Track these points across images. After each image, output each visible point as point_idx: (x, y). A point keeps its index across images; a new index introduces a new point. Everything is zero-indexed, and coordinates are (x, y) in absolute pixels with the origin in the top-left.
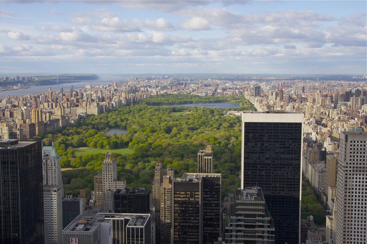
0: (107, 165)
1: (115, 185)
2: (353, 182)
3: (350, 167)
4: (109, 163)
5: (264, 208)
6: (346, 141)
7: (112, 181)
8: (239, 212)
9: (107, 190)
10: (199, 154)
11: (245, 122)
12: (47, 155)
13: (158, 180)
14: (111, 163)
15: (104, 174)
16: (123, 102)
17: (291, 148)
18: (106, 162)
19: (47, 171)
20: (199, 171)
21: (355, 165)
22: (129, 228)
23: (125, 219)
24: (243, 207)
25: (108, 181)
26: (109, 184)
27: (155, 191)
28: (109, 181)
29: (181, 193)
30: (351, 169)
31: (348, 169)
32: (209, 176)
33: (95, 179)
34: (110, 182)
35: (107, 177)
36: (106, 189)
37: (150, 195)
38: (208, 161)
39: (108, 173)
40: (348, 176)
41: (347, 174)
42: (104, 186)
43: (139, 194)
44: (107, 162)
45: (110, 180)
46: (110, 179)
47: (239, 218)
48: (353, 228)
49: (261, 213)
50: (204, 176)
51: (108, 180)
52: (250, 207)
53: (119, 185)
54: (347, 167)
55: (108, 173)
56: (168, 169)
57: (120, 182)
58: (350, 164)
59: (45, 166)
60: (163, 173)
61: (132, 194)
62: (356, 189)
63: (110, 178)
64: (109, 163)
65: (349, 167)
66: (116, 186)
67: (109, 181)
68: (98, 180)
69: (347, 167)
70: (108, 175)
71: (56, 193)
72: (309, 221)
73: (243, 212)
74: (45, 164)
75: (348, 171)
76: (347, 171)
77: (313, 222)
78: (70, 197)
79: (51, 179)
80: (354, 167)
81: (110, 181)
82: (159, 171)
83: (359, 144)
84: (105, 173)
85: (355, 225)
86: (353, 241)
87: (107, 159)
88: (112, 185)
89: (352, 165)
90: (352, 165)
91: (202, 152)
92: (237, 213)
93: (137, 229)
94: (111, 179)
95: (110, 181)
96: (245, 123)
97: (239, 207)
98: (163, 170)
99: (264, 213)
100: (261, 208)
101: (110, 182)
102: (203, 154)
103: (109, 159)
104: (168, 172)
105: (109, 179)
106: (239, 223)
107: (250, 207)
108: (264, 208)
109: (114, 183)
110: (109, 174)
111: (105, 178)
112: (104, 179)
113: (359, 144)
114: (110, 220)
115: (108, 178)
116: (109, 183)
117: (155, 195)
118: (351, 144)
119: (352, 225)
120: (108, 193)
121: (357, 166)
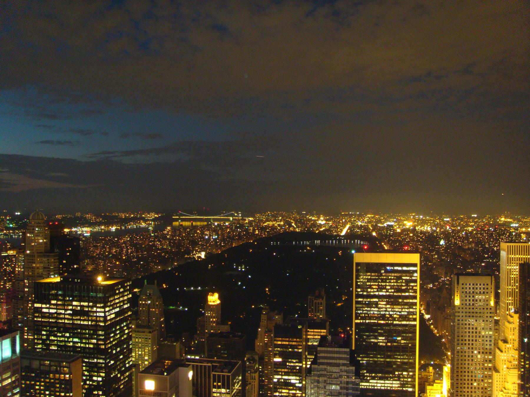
2: (466, 328)
3: (462, 312)
5: (348, 356)
6: (458, 283)
8: (321, 361)
21: (468, 310)
22: (214, 375)
23: (213, 365)
24: (326, 355)
30: (464, 314)
31: (461, 314)
40: (461, 322)
41: (459, 320)
47: (321, 366)
48: (466, 380)
49: (345, 362)
52: (333, 355)
54: (459, 312)
58: (462, 308)
62: (469, 336)
65: (461, 312)
69: (459, 312)
71: (150, 334)
72: (429, 372)
73: (325, 361)
75: (461, 316)
76: (459, 316)
77: (432, 374)
80: (466, 312)
83: (471, 286)
85: (468, 376)
86: (466, 394)
89: (464, 310)
90: (464, 310)
92: (318, 361)
93: (224, 376)
97: (321, 355)
99: (348, 362)
100: (345, 356)
106: (321, 373)
107: (333, 355)
108: (348, 356)
113: (471, 286)
114: (190, 365)
118: (463, 286)
119: (465, 376)
121: (470, 311)
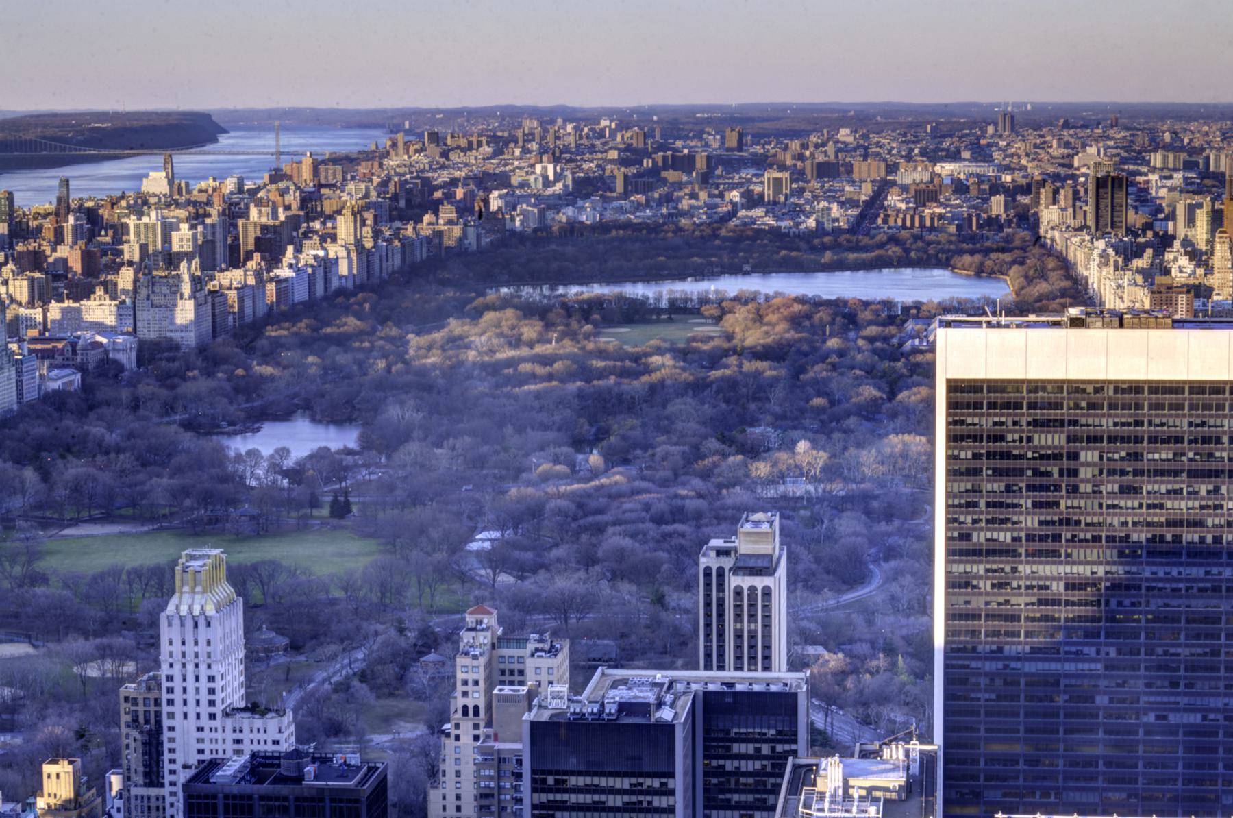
0: (189, 624)
1: (230, 736)
4: (196, 612)
7: (212, 717)
9: (185, 767)
10: (704, 562)
11: (948, 381)
13: (476, 708)
14: (210, 610)
15: (170, 678)
16: (343, 269)
17: (1210, 522)
18: (177, 607)
20: (708, 655)
25: (192, 716)
26: (200, 735)
27: (458, 774)
28: (198, 716)
29: (573, 781)
32: (739, 688)
33: (124, 706)
34: (205, 722)
35: (185, 690)
36: (180, 762)
37: (434, 797)
38: (752, 605)
39: (190, 667)
42: (172, 746)
43: (321, 790)
44: (184, 610)
45: (205, 710)
46: (204, 702)
50: (711, 687)
51: (191, 709)
53: (255, 736)
55: (190, 667)
56: (531, 646)
57: (258, 722)
60: (503, 672)
61: (283, 789)
63: (204, 697)
64: (196, 612)
66: (238, 741)
67: (198, 716)
68: (141, 709)
70: (191, 684)
81: (204, 717)
82: (482, 661)
84: (177, 671)
87: (186, 589)
88: (213, 735)
91: (721, 552)
94: (212, 703)
95: (204, 717)
96: (954, 387)
98: (506, 652)
101: (205, 722)
102: (727, 563)
103: (198, 589)
104: (530, 664)
105: (185, 703)
109: (229, 729)
111: (178, 696)
112: (171, 702)
116: (200, 729)
117: (458, 797)
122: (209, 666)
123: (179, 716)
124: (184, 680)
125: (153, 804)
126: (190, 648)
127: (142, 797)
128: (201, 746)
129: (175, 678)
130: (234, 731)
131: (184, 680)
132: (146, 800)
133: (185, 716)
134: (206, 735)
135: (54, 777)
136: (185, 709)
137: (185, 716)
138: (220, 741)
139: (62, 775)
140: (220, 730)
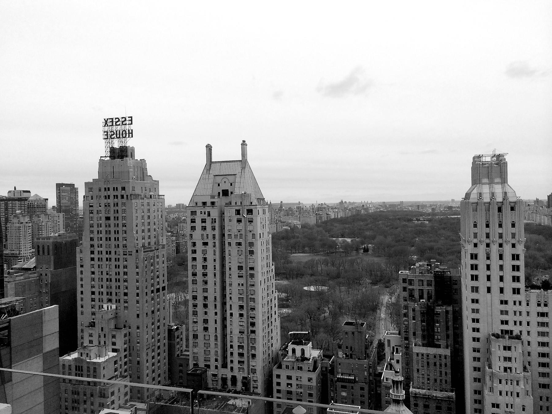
1: (534, 309)
12: (225, 193)
19: (223, 251)
26: (503, 307)
28: (502, 290)
34: (508, 295)
45: (509, 285)
46: (508, 278)
51: (495, 284)
59: (217, 232)
63: (508, 274)
67: (502, 290)
70: (495, 262)
74: (217, 225)
78: (303, 351)
79: (236, 281)
88: (517, 308)
101: (508, 295)
109: (533, 303)
110: (501, 257)
115: (495, 273)
120: (508, 354)
122: (514, 246)
123: (483, 290)
124: (488, 258)
125: (432, 361)
126: (495, 230)
127: (423, 355)
128: (505, 317)
129: (479, 257)
130: (539, 305)
131: (488, 258)
132: (425, 357)
133: (489, 290)
134: (510, 307)
135: (350, 334)
136: (501, 285)
137: (489, 290)
138: (524, 314)
139: (356, 333)
140: (524, 303)
